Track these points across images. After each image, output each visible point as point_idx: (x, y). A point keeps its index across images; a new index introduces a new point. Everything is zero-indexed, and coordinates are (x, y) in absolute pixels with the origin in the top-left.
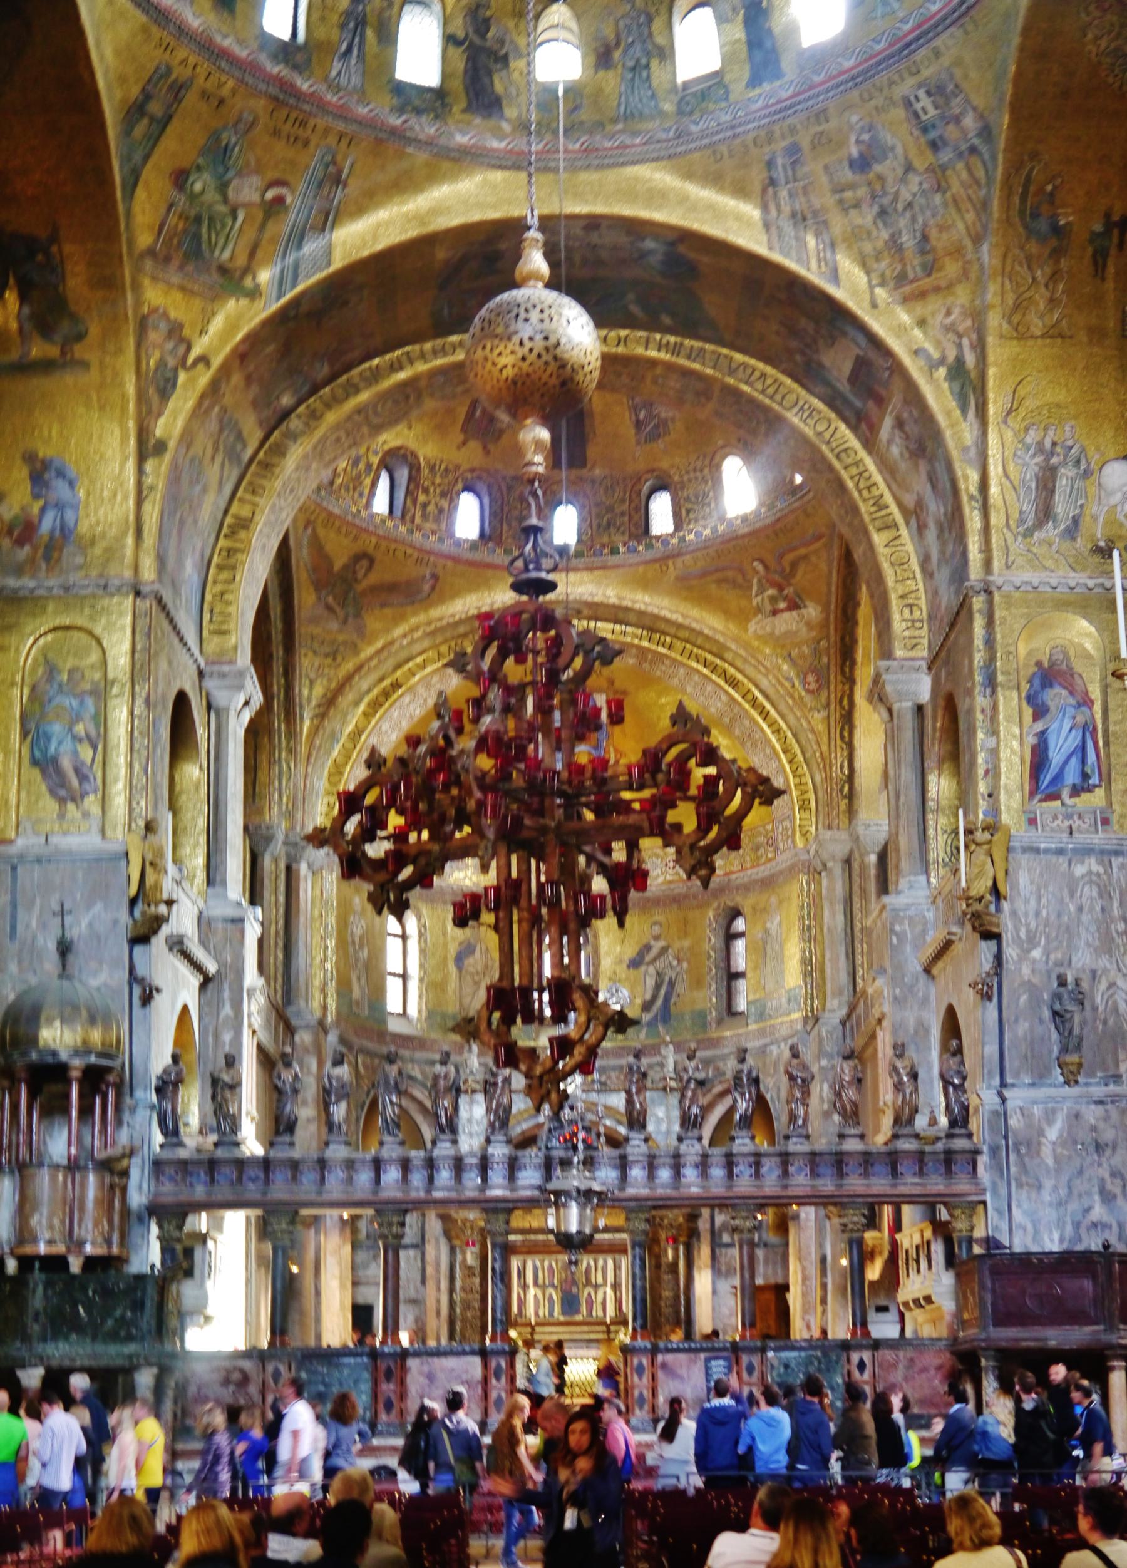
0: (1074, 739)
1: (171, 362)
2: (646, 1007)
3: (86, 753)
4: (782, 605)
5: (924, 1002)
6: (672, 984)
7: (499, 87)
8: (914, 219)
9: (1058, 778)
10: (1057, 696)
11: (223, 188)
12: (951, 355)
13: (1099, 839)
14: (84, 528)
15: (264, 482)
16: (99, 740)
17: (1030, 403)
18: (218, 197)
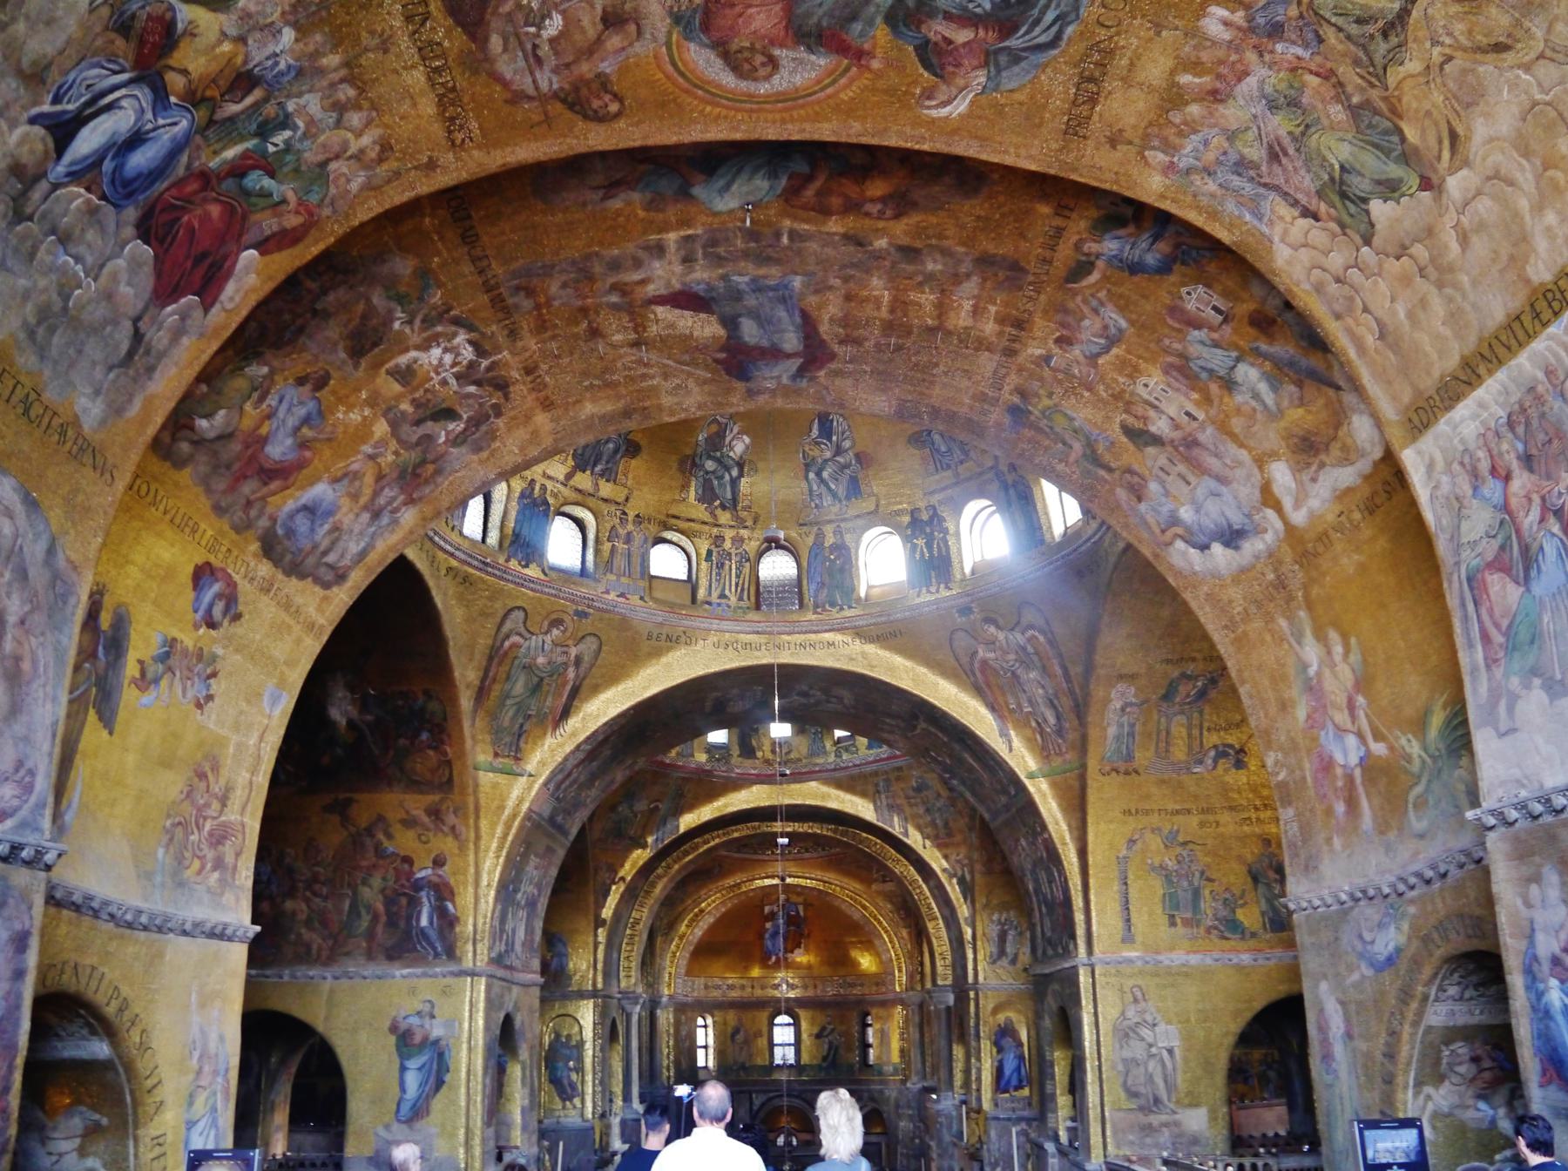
2: (825, 1059)
3: (574, 1076)
5: (952, 1157)
6: (837, 1049)
7: (754, 743)
9: (1009, 1082)
10: (1007, 1042)
13: (1026, 1113)
14: (571, 965)
16: (580, 1069)
17: (995, 902)
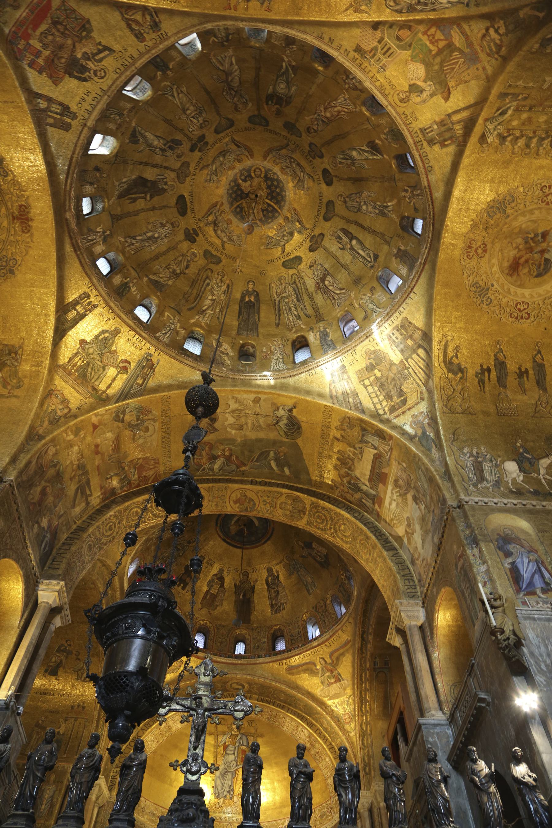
0: (532, 567)
1: (59, 413)
4: (332, 681)
8: (396, 384)
9: (531, 583)
11: (102, 355)
12: (420, 432)
15: (97, 516)
18: (99, 358)
